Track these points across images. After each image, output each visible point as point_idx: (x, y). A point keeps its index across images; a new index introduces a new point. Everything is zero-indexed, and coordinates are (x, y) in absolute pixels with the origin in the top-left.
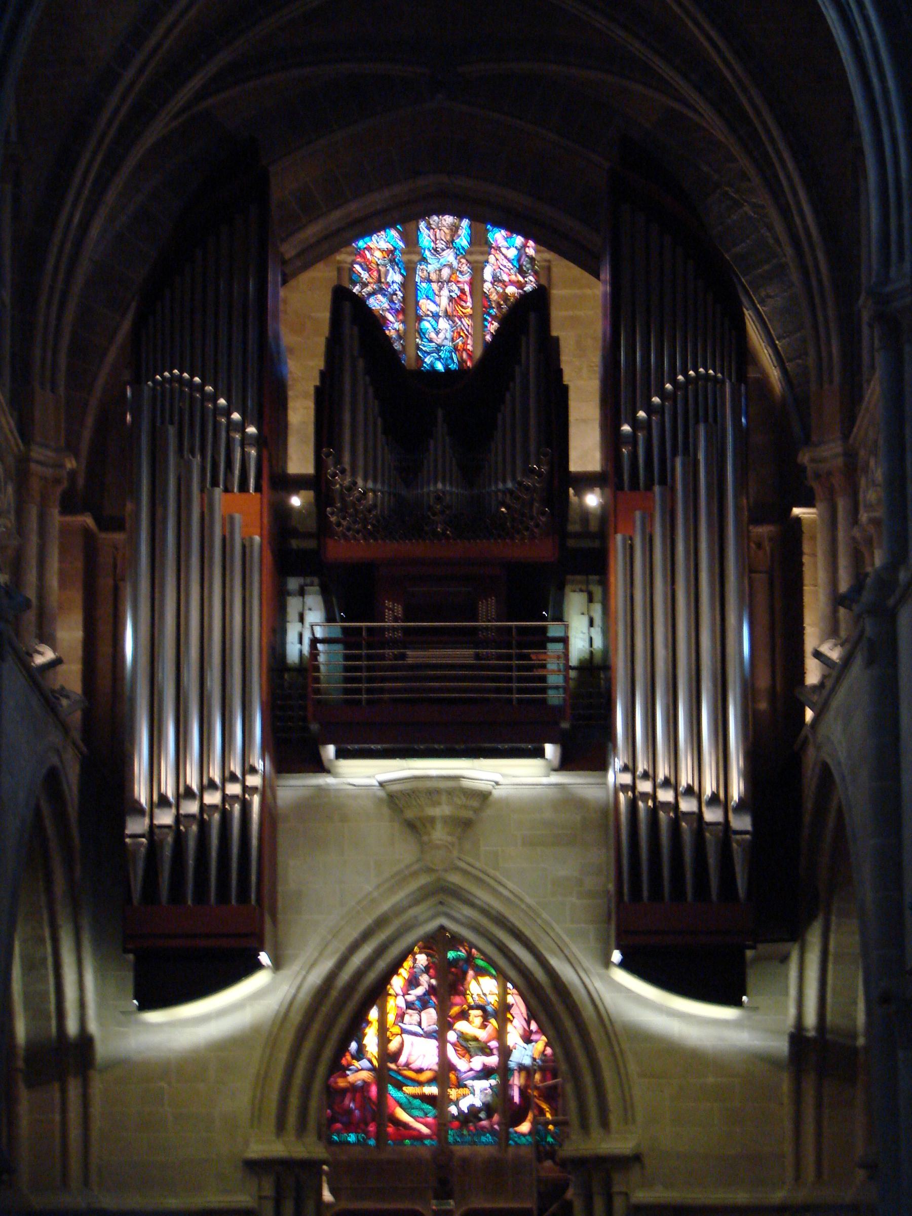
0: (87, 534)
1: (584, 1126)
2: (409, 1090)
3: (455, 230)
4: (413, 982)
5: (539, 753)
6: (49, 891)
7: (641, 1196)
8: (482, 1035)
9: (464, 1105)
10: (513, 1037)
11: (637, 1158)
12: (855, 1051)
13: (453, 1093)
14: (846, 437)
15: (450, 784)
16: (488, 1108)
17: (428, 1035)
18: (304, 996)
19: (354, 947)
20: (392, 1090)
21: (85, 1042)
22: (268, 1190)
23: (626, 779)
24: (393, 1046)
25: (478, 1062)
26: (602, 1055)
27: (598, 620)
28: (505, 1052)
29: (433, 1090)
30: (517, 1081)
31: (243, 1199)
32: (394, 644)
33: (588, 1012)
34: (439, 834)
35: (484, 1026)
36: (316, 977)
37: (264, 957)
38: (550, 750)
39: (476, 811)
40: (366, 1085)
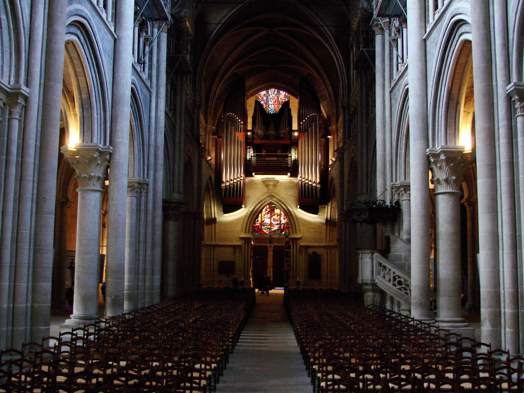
0: (216, 139)
1: (293, 233)
2: (265, 227)
3: (275, 91)
4: (266, 210)
5: (287, 174)
6: (210, 195)
7: (302, 244)
8: (277, 218)
9: (274, 229)
10: (282, 218)
11: (301, 238)
12: (336, 222)
13: (272, 227)
14: (336, 124)
15: (273, 179)
16: (278, 230)
17: (269, 218)
18: (249, 212)
19: (257, 205)
20: (263, 227)
21: (215, 219)
22: (243, 242)
23: (301, 179)
24: (263, 220)
25: (276, 223)
26: (296, 222)
27: (296, 153)
28: (281, 221)
29: (269, 227)
30: (282, 226)
31: (239, 243)
32: (264, 157)
33: (294, 215)
34: (271, 187)
35: (277, 217)
36: (251, 209)
37: (243, 206)
38: (289, 174)
39: (277, 183)
40: (259, 226)
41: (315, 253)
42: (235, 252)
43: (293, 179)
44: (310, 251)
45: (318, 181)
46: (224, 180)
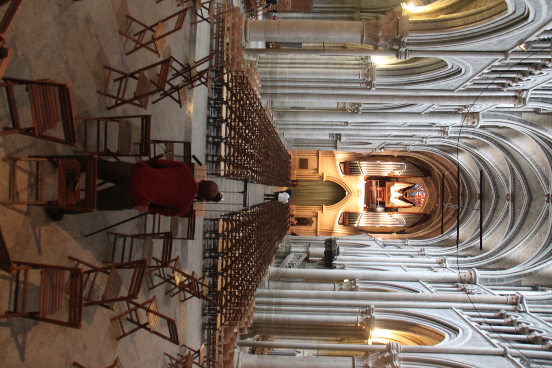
34: (357, 193)
41: (313, 222)
42: (314, 169)
43: (363, 208)
44: (314, 219)
45: (360, 225)
46: (361, 163)
